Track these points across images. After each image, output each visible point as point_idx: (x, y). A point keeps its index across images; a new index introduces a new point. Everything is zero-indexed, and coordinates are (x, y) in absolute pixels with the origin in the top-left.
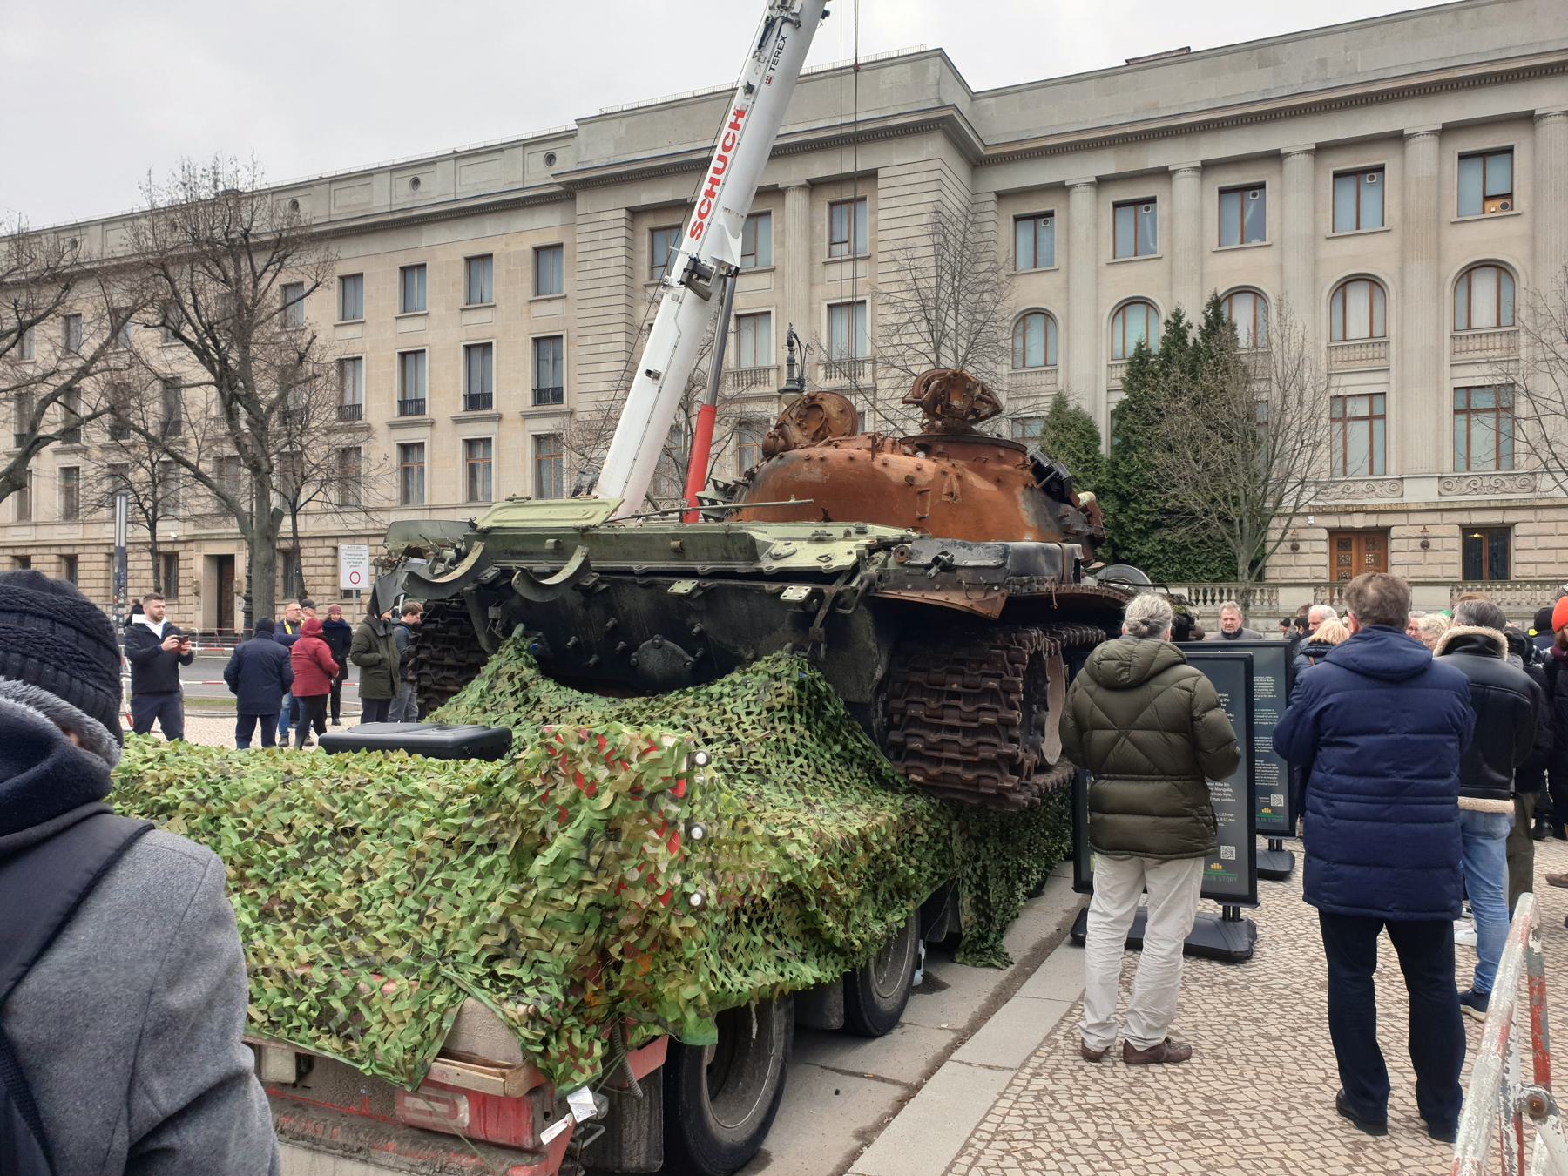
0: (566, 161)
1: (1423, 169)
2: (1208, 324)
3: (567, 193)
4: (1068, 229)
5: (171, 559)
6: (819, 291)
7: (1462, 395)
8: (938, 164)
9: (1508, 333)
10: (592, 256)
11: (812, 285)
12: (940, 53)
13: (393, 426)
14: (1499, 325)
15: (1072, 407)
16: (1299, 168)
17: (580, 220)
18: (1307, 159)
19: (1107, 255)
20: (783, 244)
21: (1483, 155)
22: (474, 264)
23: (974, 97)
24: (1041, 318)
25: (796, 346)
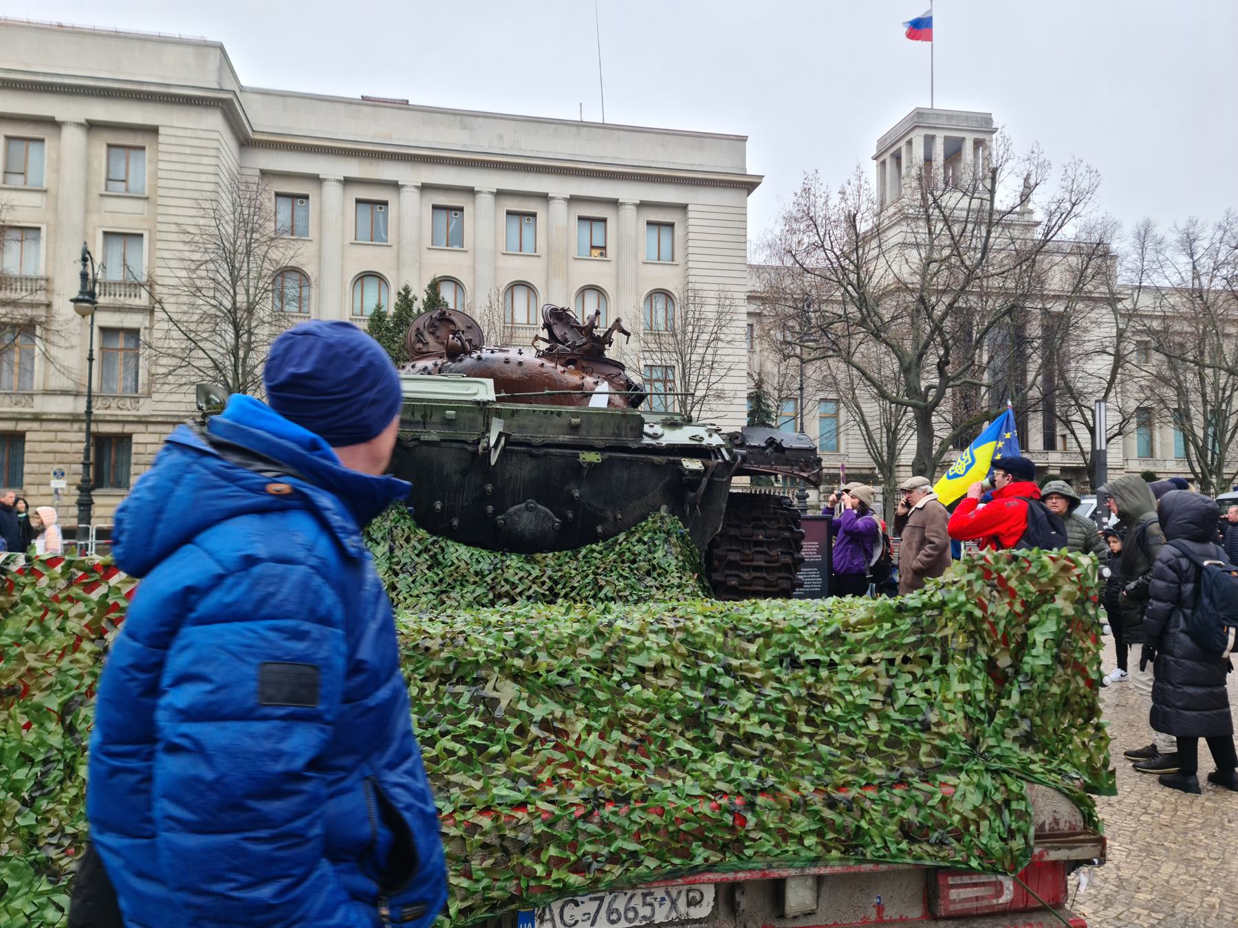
1: (558, 221)
2: (429, 298)
4: (321, 212)
6: (94, 219)
8: (216, 136)
11: (87, 211)
16: (485, 201)
18: (491, 197)
19: (350, 237)
20: (57, 171)
21: (592, 220)
23: (242, 89)
24: (296, 276)
25: (89, 263)
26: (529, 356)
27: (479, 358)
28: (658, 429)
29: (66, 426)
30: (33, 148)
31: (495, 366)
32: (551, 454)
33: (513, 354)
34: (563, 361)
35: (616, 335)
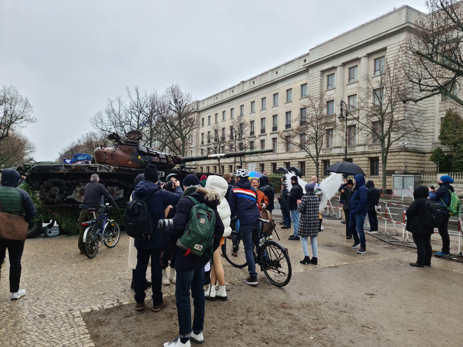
0: (310, 60)
3: (306, 70)
5: (223, 167)
10: (312, 85)
12: (407, 7)
13: (271, 134)
17: (310, 76)
22: (289, 91)
29: (337, 157)
30: (356, 68)
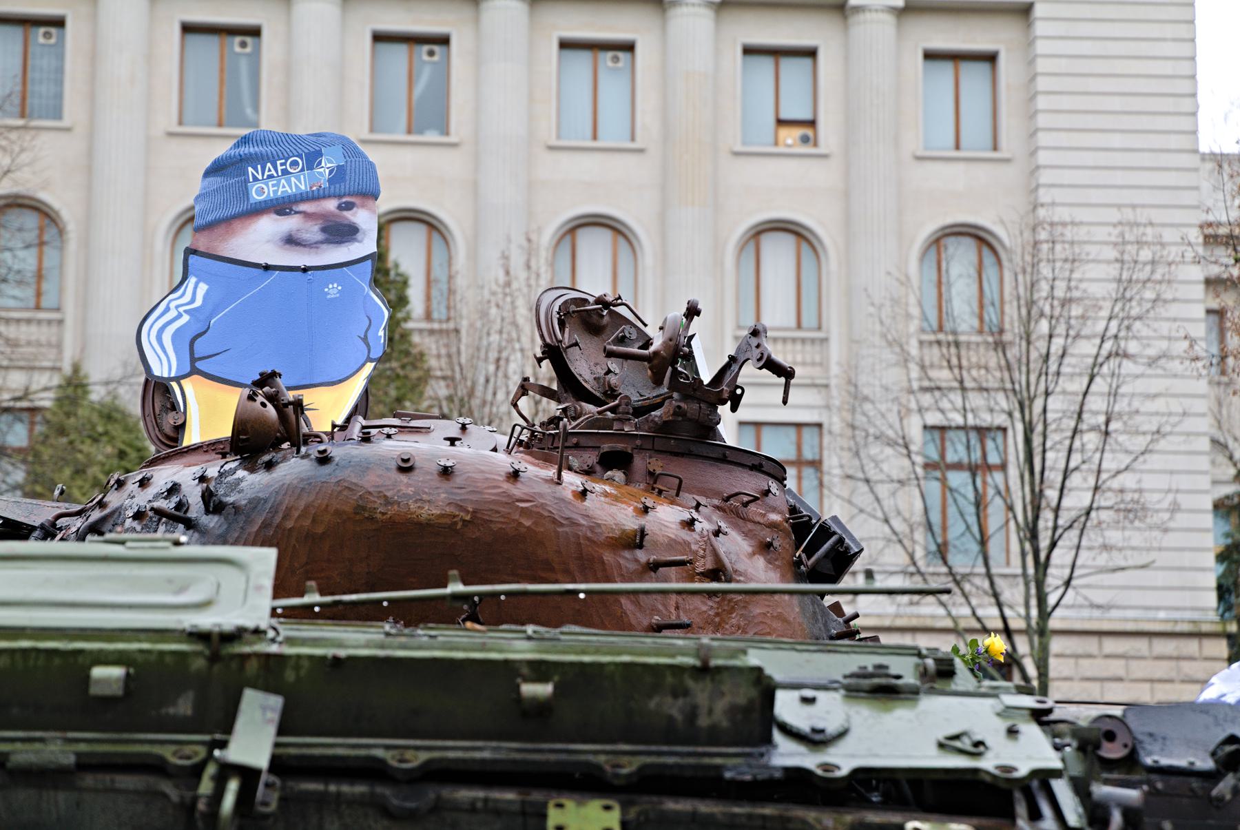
4: (94, 58)
7: (750, 431)
9: (813, 341)
14: (799, 326)
15: (97, 394)
19: (167, 118)
26: (485, 453)
27: (324, 459)
28: (830, 711)
31: (370, 481)
32: (456, 807)
33: (429, 447)
34: (591, 458)
35: (749, 373)
